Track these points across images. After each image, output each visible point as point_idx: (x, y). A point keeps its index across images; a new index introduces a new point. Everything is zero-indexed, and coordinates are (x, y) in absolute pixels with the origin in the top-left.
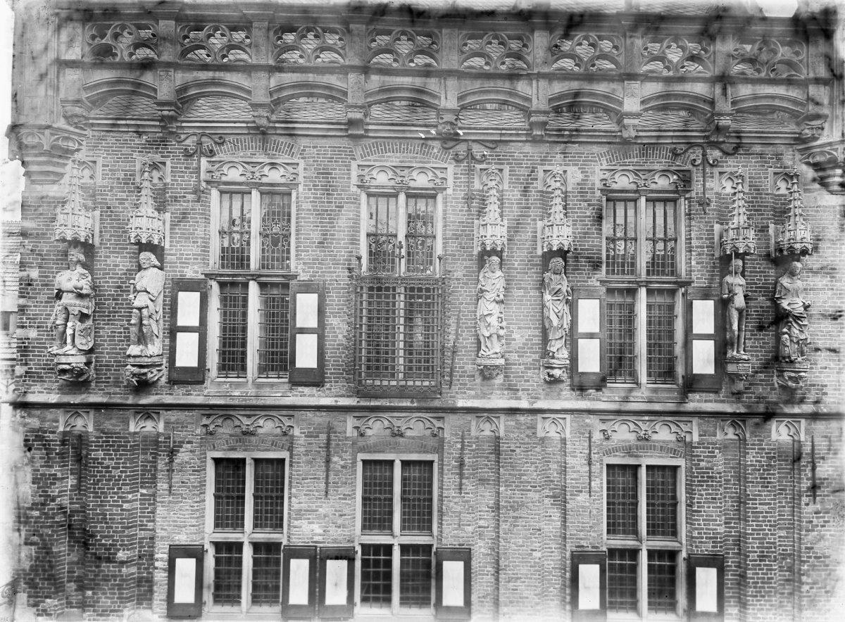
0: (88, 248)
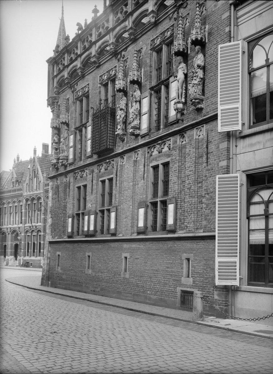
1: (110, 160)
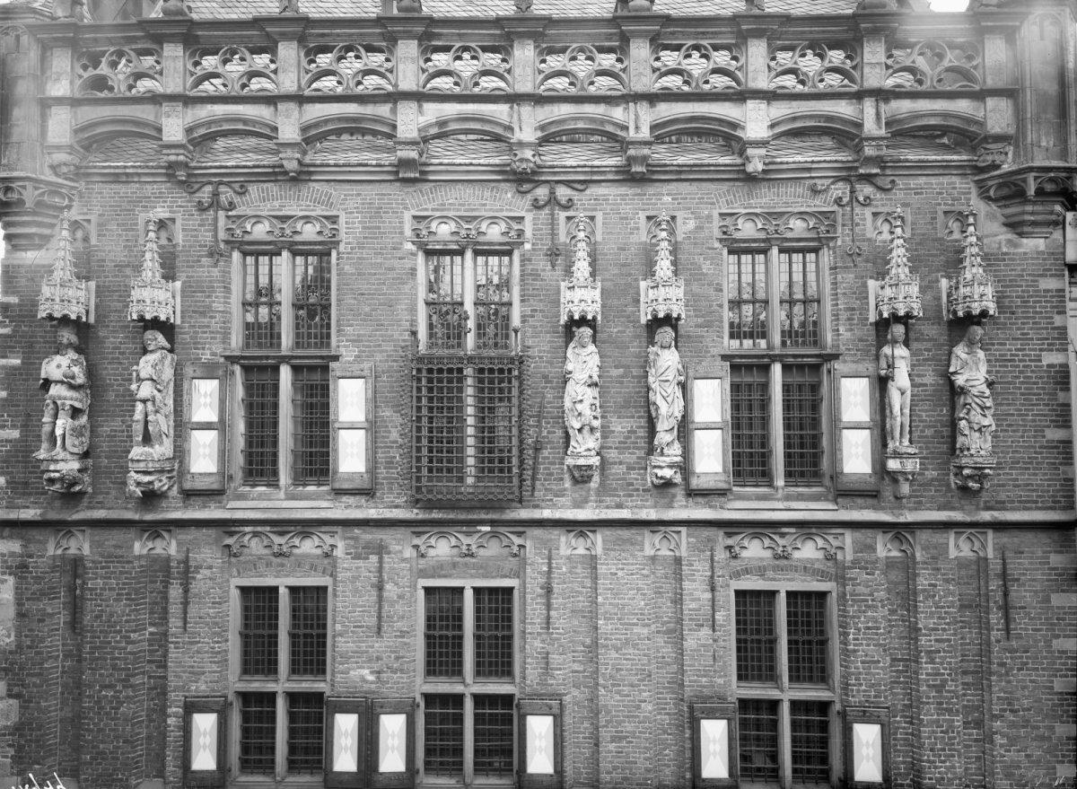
1: (502, 529)
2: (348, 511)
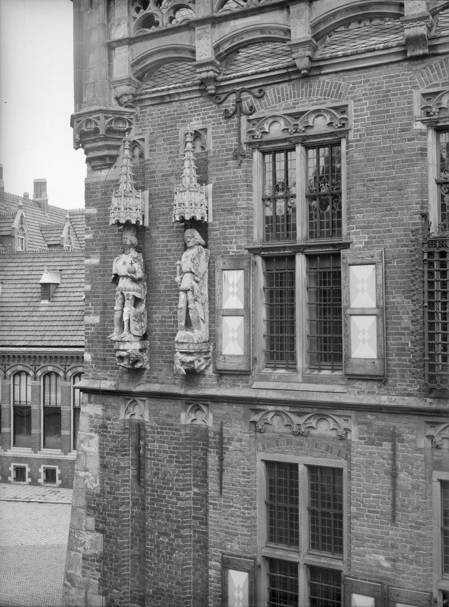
0: (139, 229)
2: (360, 397)
